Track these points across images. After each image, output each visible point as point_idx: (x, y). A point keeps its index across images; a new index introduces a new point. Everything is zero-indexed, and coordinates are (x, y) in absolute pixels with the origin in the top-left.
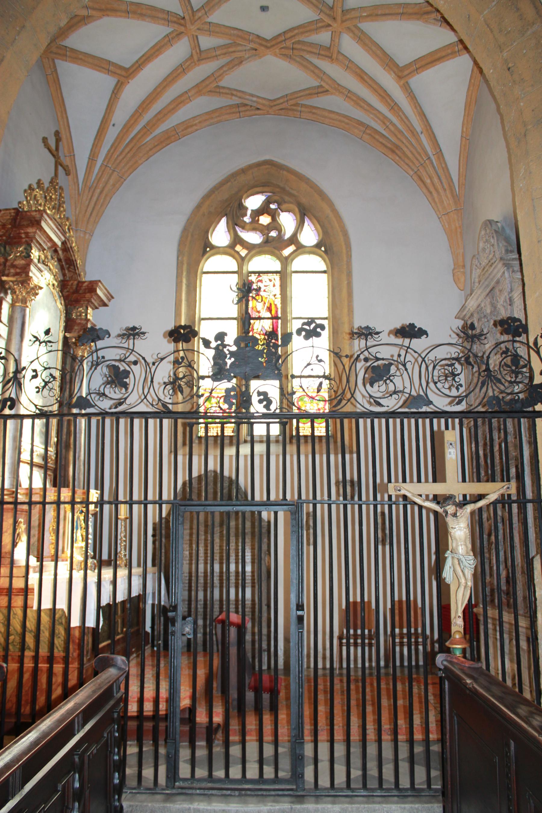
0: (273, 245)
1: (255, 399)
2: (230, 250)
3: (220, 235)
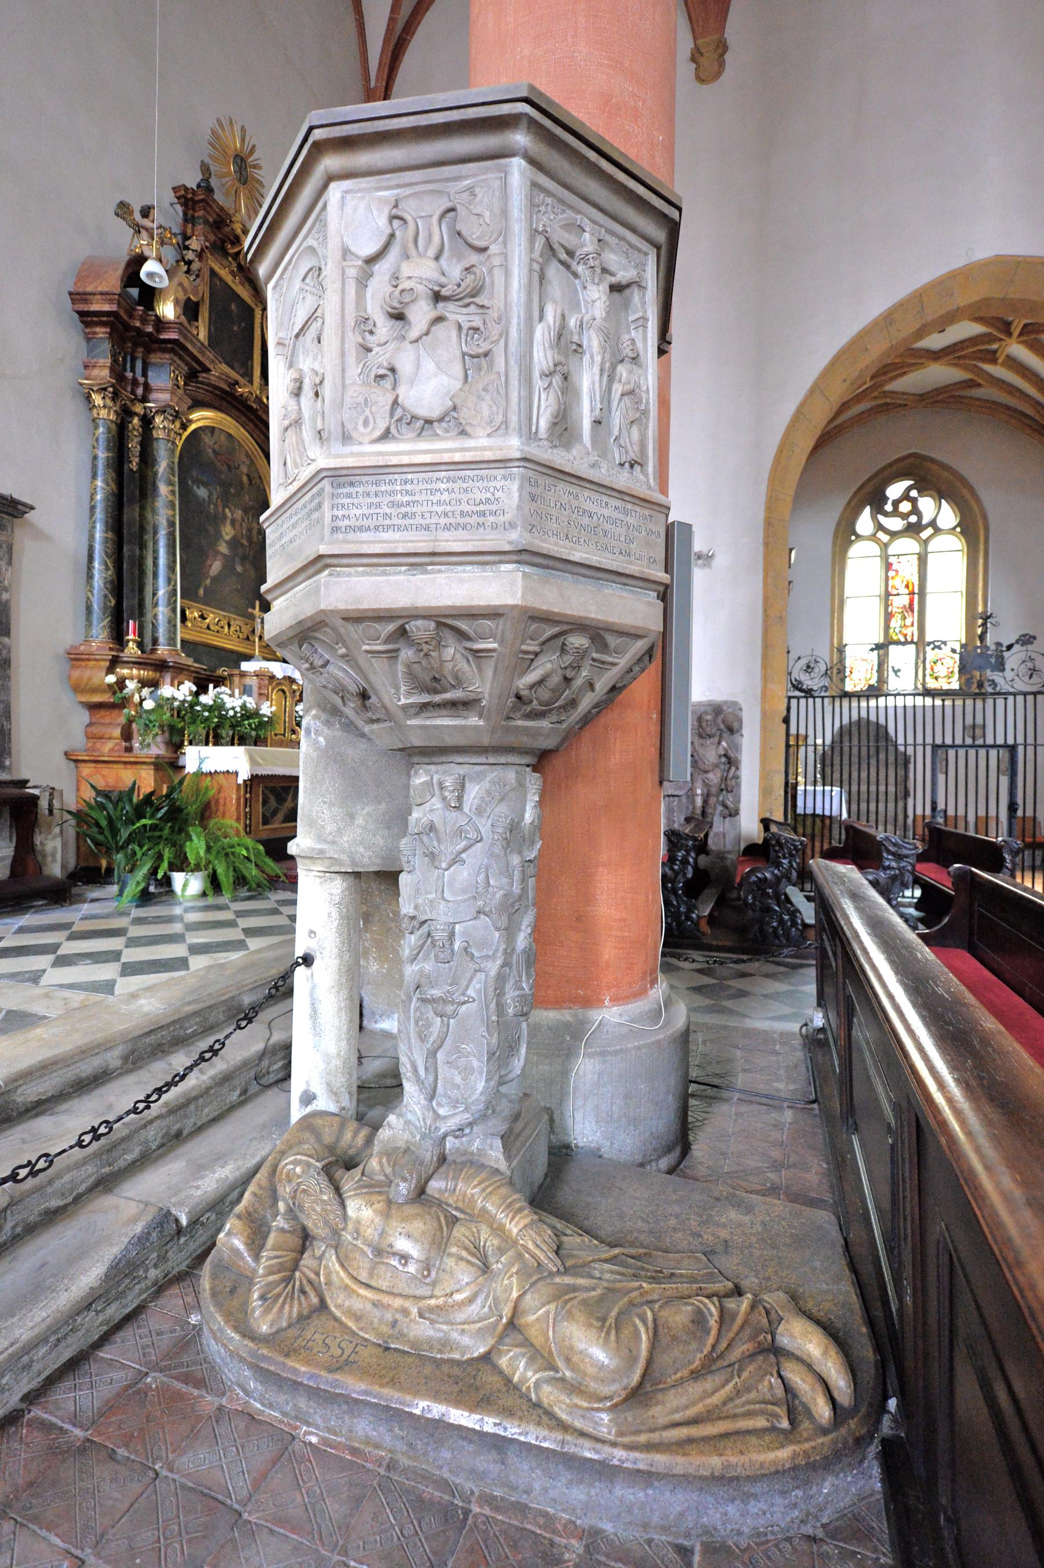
0: (913, 530)
1: (986, 684)
2: (873, 537)
3: (864, 523)
